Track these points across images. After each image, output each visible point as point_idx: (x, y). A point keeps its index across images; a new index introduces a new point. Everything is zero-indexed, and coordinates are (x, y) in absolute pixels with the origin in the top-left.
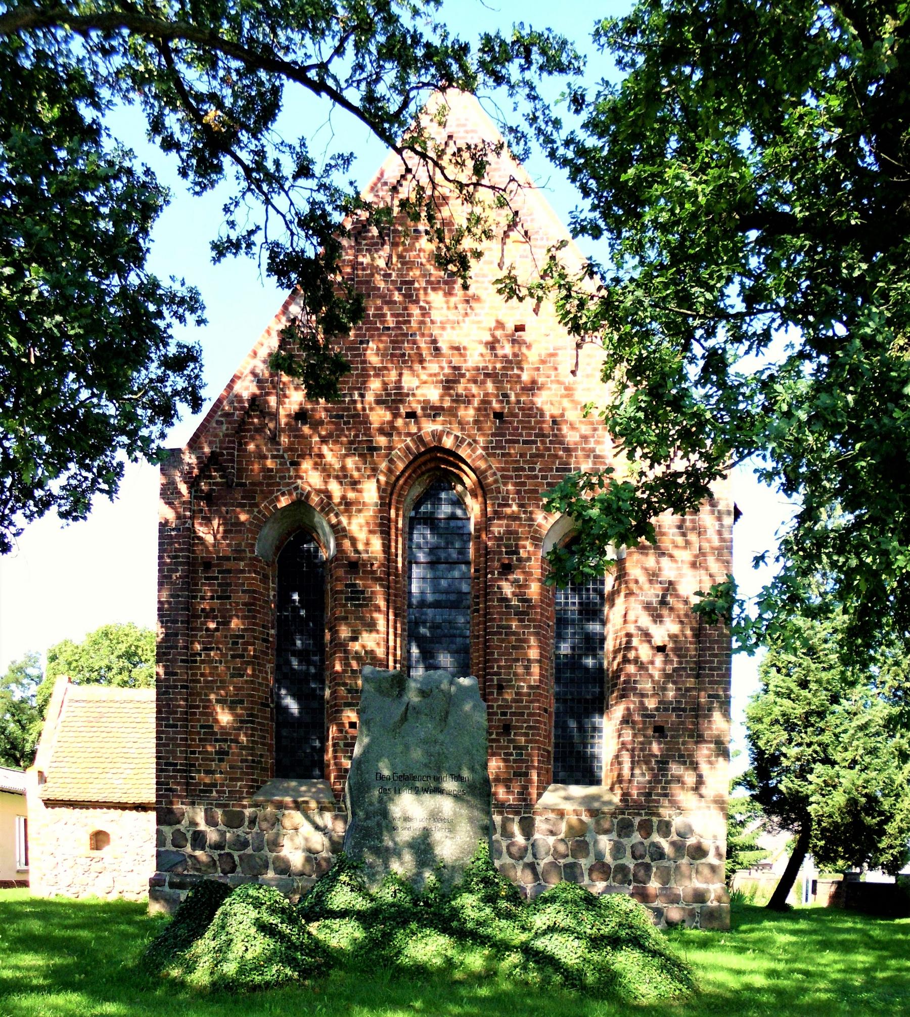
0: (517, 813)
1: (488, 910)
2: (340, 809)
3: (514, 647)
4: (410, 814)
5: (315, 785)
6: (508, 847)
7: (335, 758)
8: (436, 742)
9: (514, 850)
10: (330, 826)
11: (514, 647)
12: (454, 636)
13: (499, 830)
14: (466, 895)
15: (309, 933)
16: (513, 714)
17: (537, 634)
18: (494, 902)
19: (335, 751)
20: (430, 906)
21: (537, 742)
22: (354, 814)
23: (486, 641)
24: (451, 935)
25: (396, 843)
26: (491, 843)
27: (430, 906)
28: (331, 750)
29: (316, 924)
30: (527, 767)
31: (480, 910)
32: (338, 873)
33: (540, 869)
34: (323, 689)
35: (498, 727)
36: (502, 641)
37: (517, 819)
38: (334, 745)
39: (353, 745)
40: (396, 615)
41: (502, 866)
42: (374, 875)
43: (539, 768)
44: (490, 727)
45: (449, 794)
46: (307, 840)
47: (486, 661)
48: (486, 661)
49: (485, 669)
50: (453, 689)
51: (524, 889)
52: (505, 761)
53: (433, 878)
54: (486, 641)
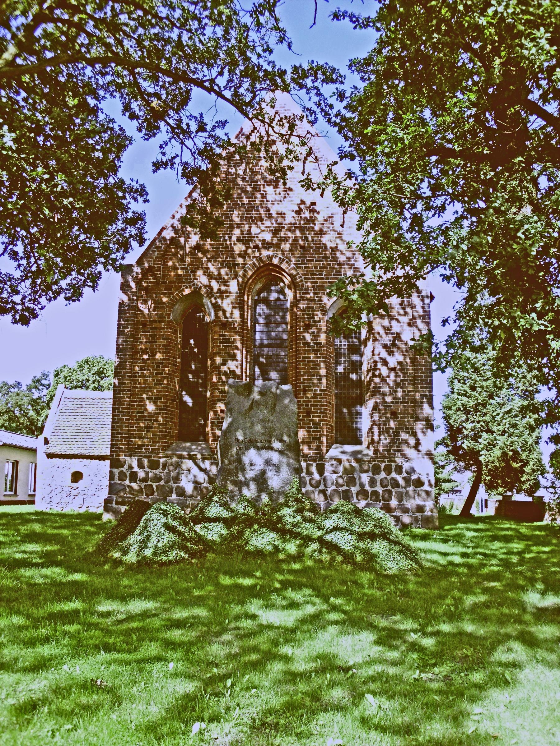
0: (315, 461)
1: (299, 518)
2: (215, 459)
3: (312, 369)
4: (254, 461)
5: (200, 445)
6: (310, 480)
7: (212, 430)
8: (269, 421)
9: (313, 482)
10: (208, 469)
11: (312, 369)
12: (279, 362)
13: (305, 471)
14: (286, 508)
15: (195, 531)
16: (312, 405)
17: (324, 361)
18: (302, 513)
19: (212, 426)
20: (265, 515)
21: (326, 420)
22: (222, 461)
23: (297, 365)
24: (277, 532)
25: (246, 478)
26: (300, 478)
27: (265, 515)
28: (210, 425)
29: (199, 526)
30: (321, 435)
31: (294, 517)
32: (212, 496)
33: (328, 493)
34: (206, 392)
35: (303, 413)
36: (305, 365)
37: (315, 464)
38: (212, 423)
39: (222, 422)
40: (247, 351)
41: (307, 491)
42: (233, 497)
43: (327, 436)
44: (299, 412)
45: (276, 450)
46: (195, 476)
47: (297, 376)
48: (297, 376)
49: (296, 380)
50: (278, 391)
51: (319, 505)
52: (308, 431)
53: (267, 498)
54: (297, 365)
